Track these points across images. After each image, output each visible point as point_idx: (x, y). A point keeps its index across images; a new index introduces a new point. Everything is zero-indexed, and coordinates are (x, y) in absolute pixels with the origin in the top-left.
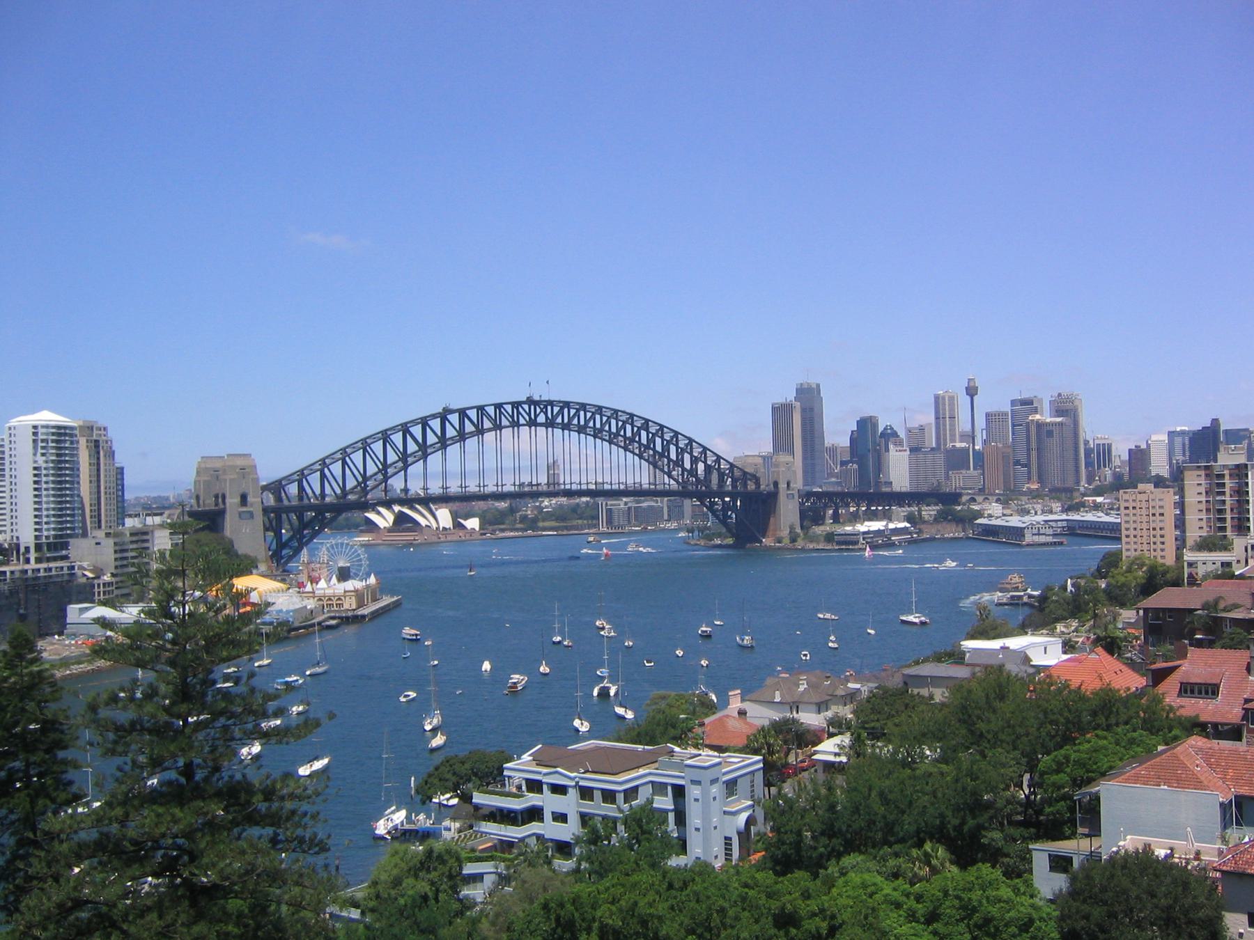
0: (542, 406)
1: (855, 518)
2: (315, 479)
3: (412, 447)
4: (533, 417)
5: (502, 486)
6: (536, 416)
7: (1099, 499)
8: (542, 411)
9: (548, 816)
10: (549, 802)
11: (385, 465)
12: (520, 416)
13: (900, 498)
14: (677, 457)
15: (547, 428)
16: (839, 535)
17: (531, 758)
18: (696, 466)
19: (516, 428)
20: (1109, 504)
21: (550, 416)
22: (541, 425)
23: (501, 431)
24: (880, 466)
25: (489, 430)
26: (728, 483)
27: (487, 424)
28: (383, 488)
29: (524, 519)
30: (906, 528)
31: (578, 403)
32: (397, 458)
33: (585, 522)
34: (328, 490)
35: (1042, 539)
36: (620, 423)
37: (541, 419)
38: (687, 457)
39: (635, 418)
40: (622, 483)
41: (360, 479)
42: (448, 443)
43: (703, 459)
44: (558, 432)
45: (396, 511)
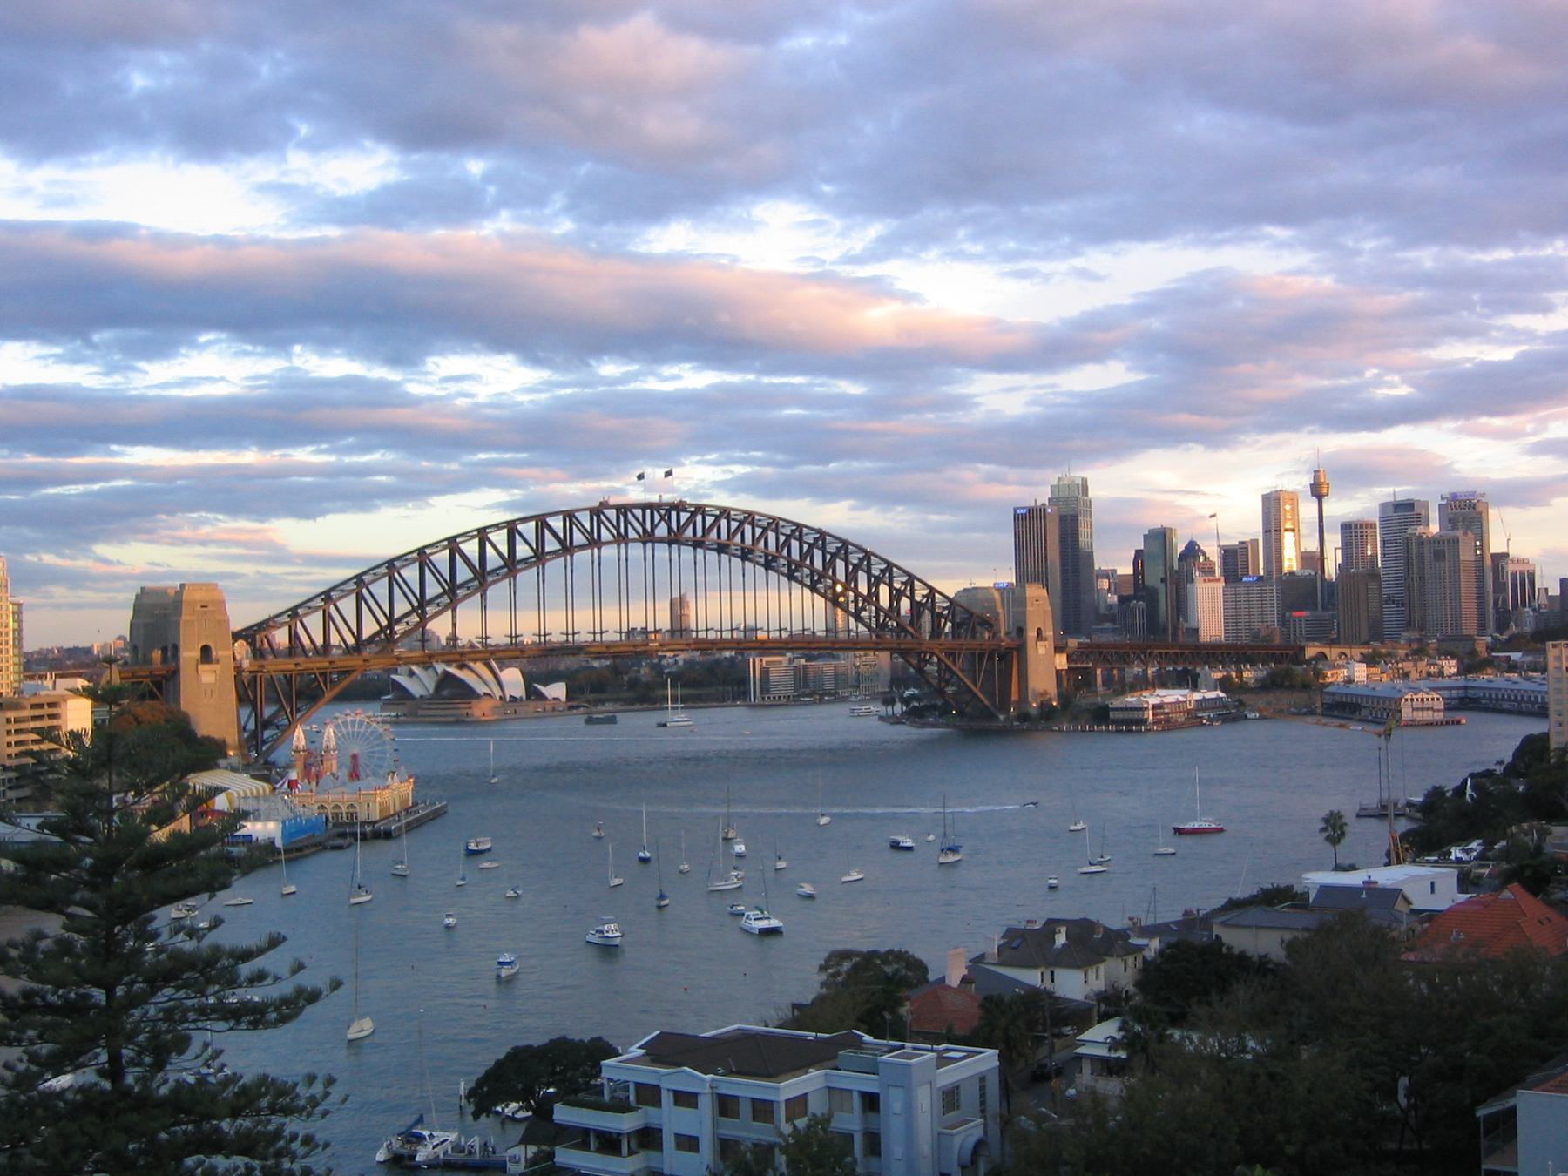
0: (663, 512)
1: (1143, 684)
2: (314, 622)
3: (463, 574)
4: (648, 527)
5: (601, 633)
6: (653, 527)
7: (1515, 656)
8: (662, 518)
9: (668, 1140)
10: (672, 1120)
11: (423, 602)
12: (629, 527)
13: (1214, 654)
14: (869, 590)
15: (670, 545)
16: (1117, 709)
17: (644, 1051)
18: (898, 603)
19: (623, 545)
20: (1531, 662)
21: (674, 525)
22: (661, 540)
23: (599, 549)
24: (1181, 605)
25: (582, 547)
26: (947, 630)
27: (579, 538)
28: (419, 637)
29: (634, 684)
30: (1219, 698)
31: (718, 508)
32: (441, 591)
33: (730, 688)
34: (335, 639)
35: (1428, 716)
36: (782, 538)
37: (662, 531)
38: (884, 591)
39: (805, 530)
40: (786, 629)
41: (384, 622)
42: (519, 567)
43: (908, 594)
44: (687, 552)
45: (439, 672)
